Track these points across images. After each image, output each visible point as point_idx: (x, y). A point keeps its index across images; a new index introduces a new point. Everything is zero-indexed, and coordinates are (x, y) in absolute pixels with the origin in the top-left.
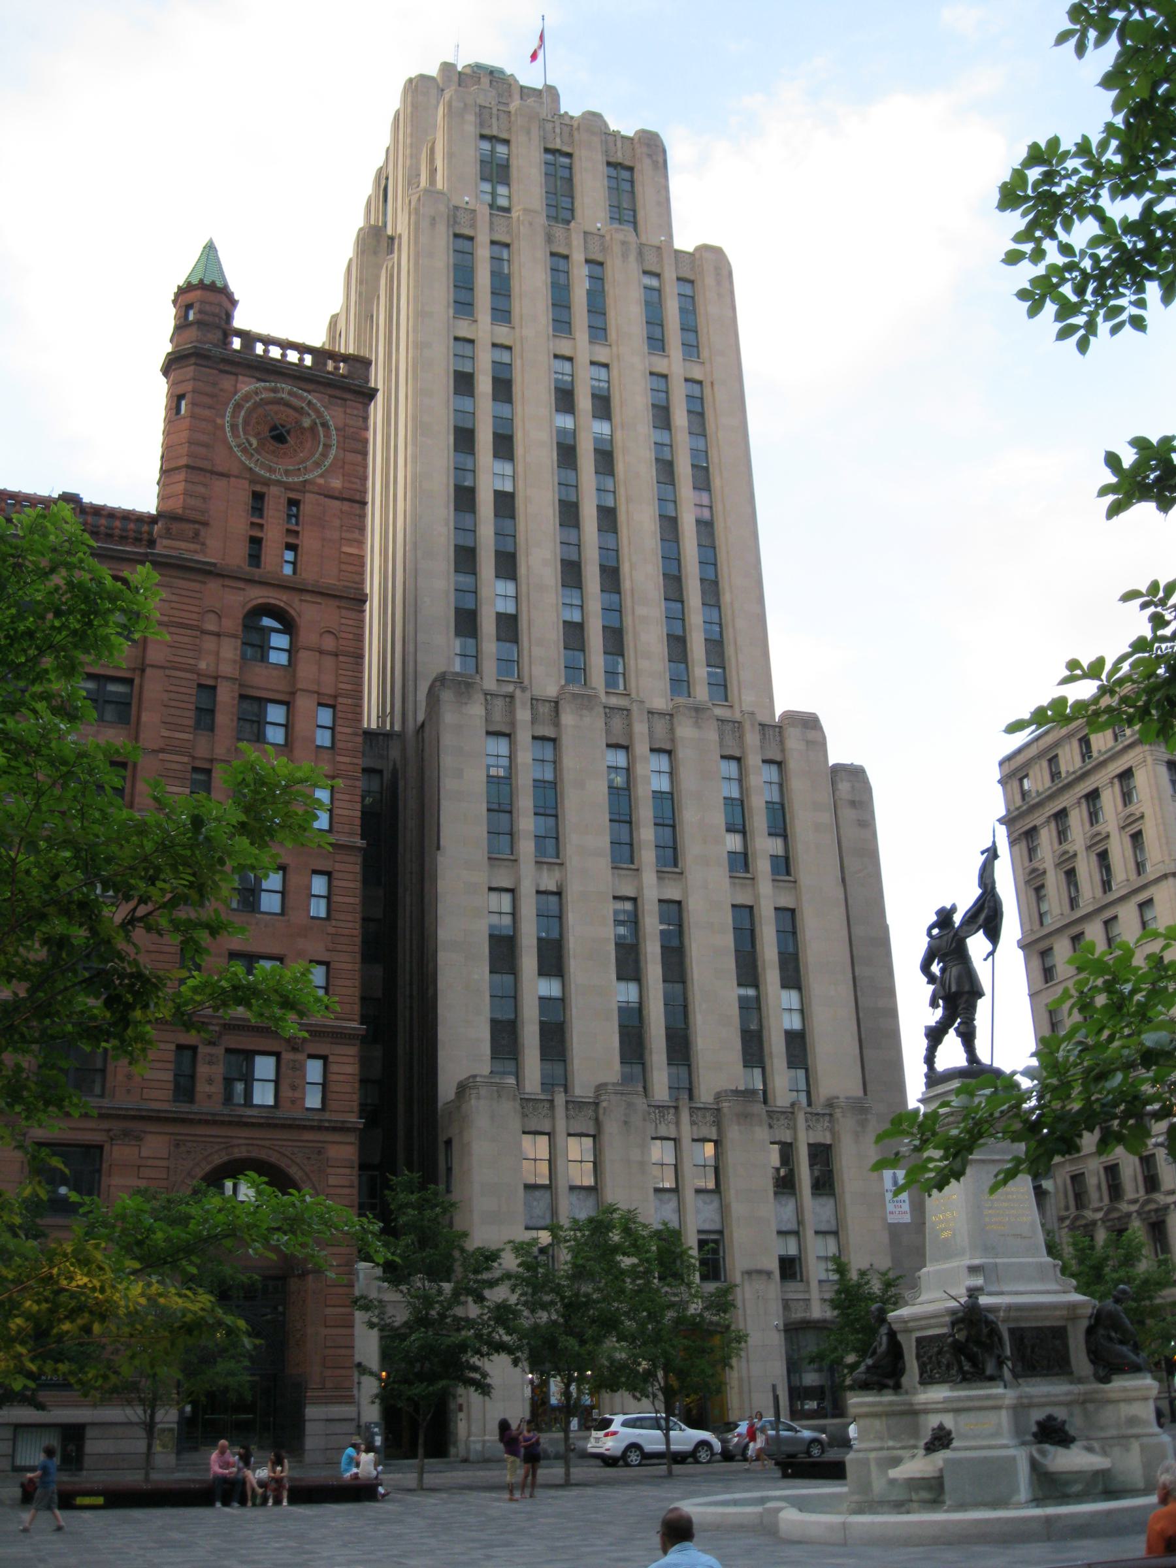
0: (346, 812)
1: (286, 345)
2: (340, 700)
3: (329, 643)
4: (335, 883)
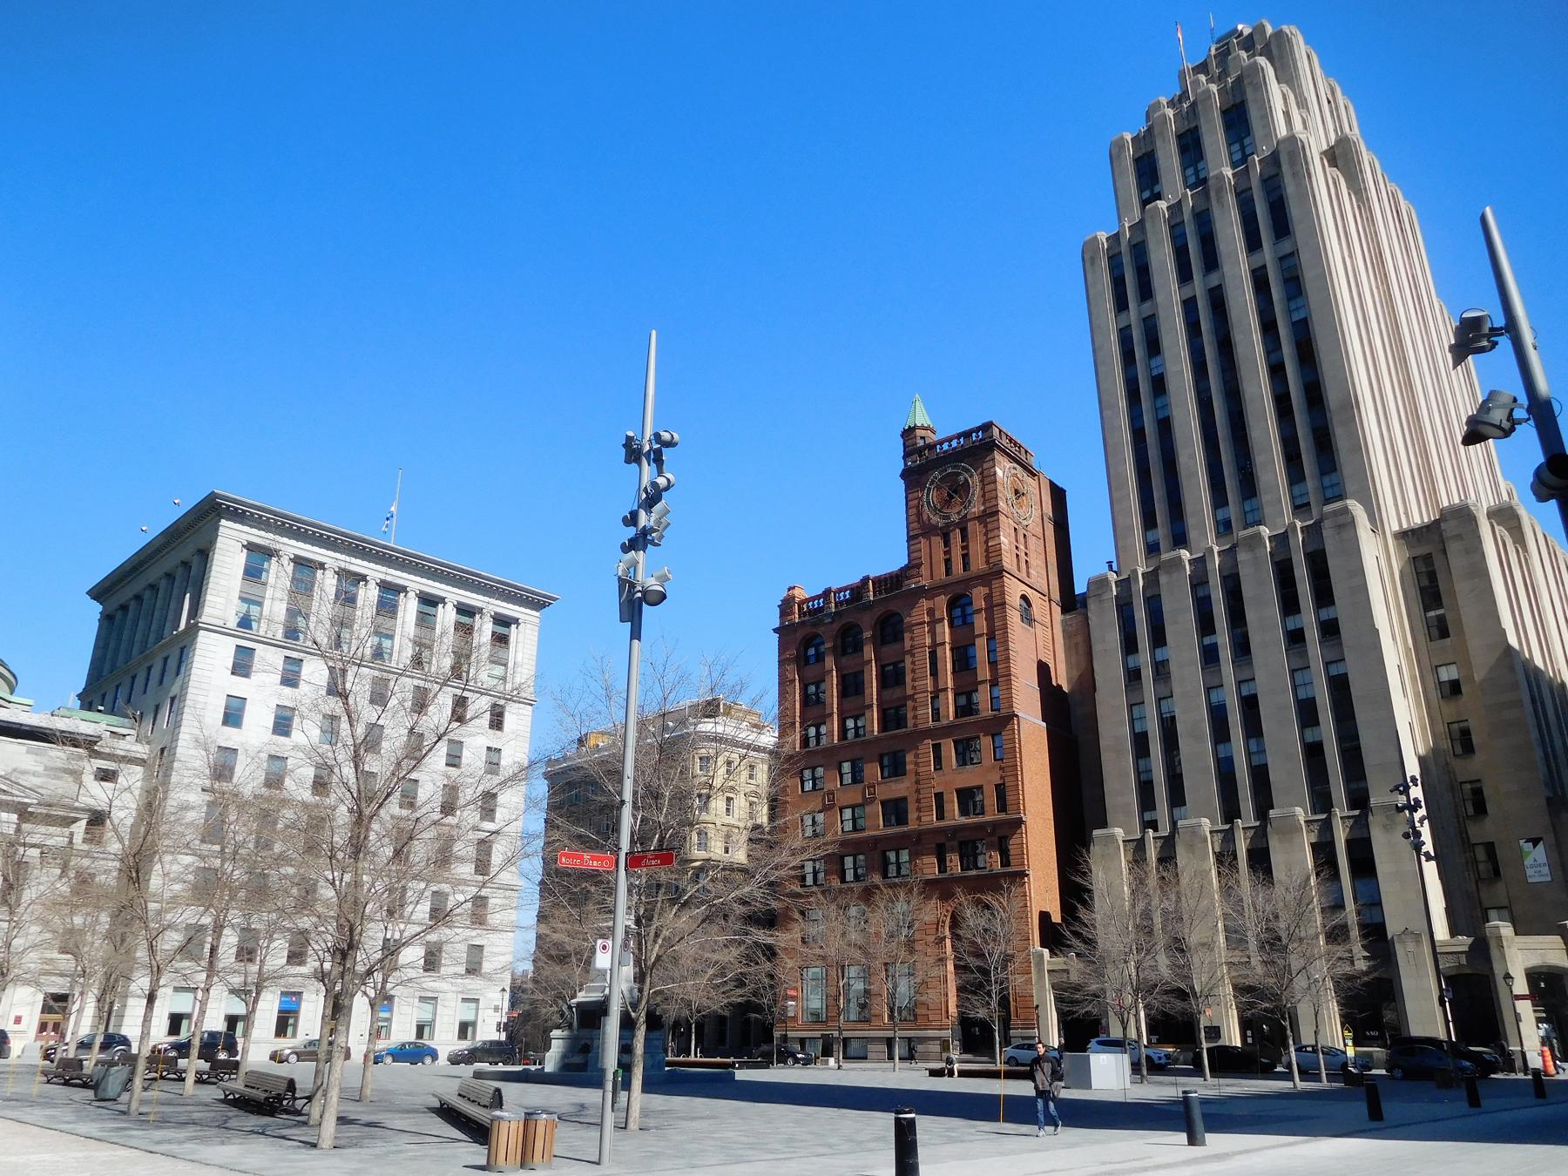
1: (949, 440)
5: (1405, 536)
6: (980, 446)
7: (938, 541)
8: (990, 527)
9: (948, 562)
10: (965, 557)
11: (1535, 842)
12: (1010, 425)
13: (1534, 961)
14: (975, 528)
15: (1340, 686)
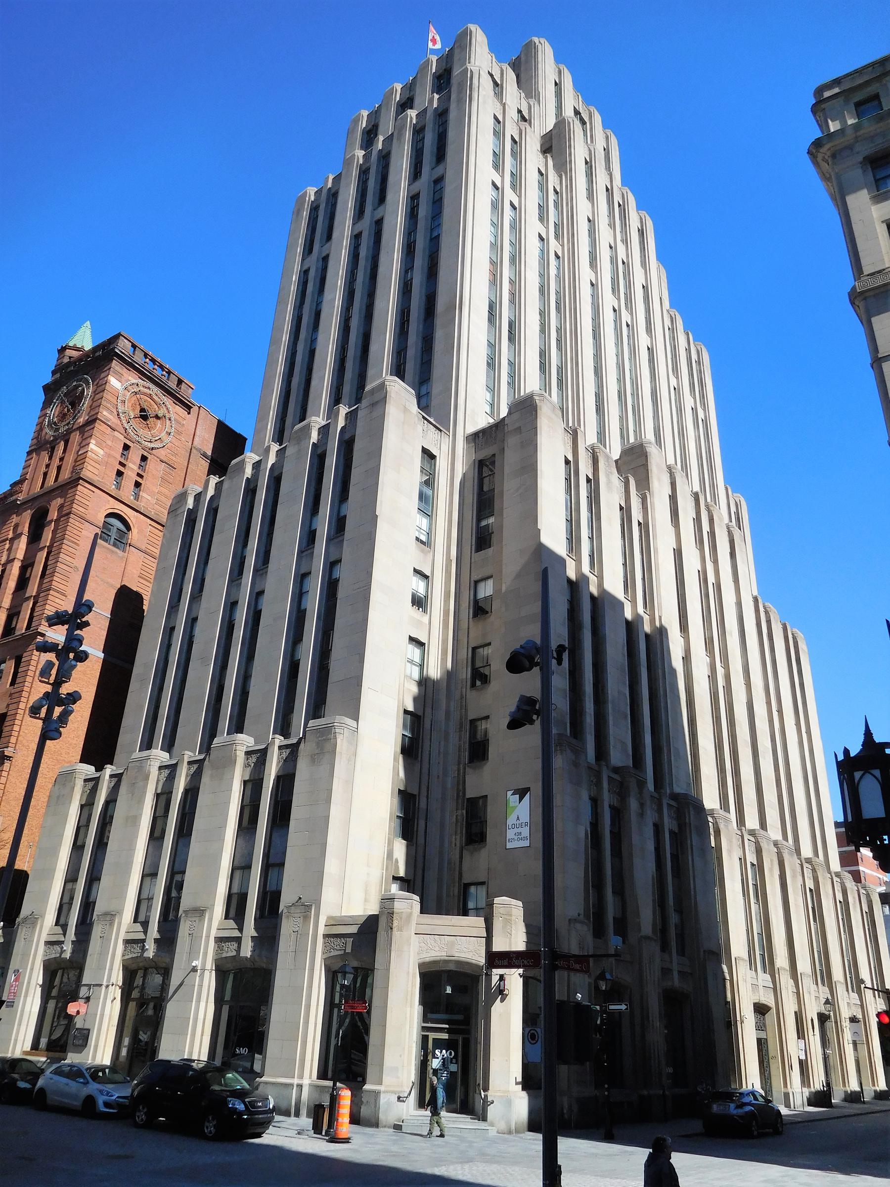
5: (476, 438)
6: (103, 356)
7: (45, 456)
8: (86, 435)
9: (45, 474)
10: (59, 468)
11: (522, 793)
12: (140, 334)
13: (437, 950)
14: (76, 437)
15: (331, 587)
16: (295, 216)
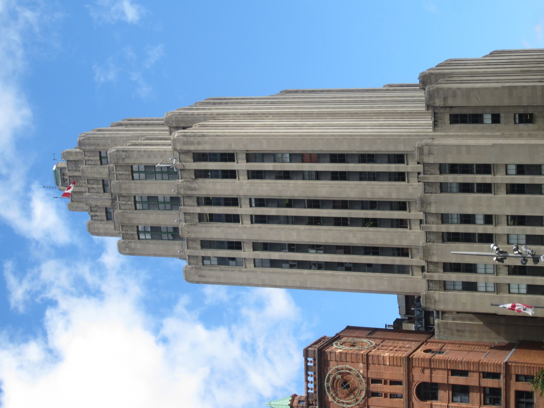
0: (492, 368)
1: (307, 382)
2: (449, 368)
3: (427, 372)
4: (520, 373)
10: (393, 383)
16: (204, 279)
